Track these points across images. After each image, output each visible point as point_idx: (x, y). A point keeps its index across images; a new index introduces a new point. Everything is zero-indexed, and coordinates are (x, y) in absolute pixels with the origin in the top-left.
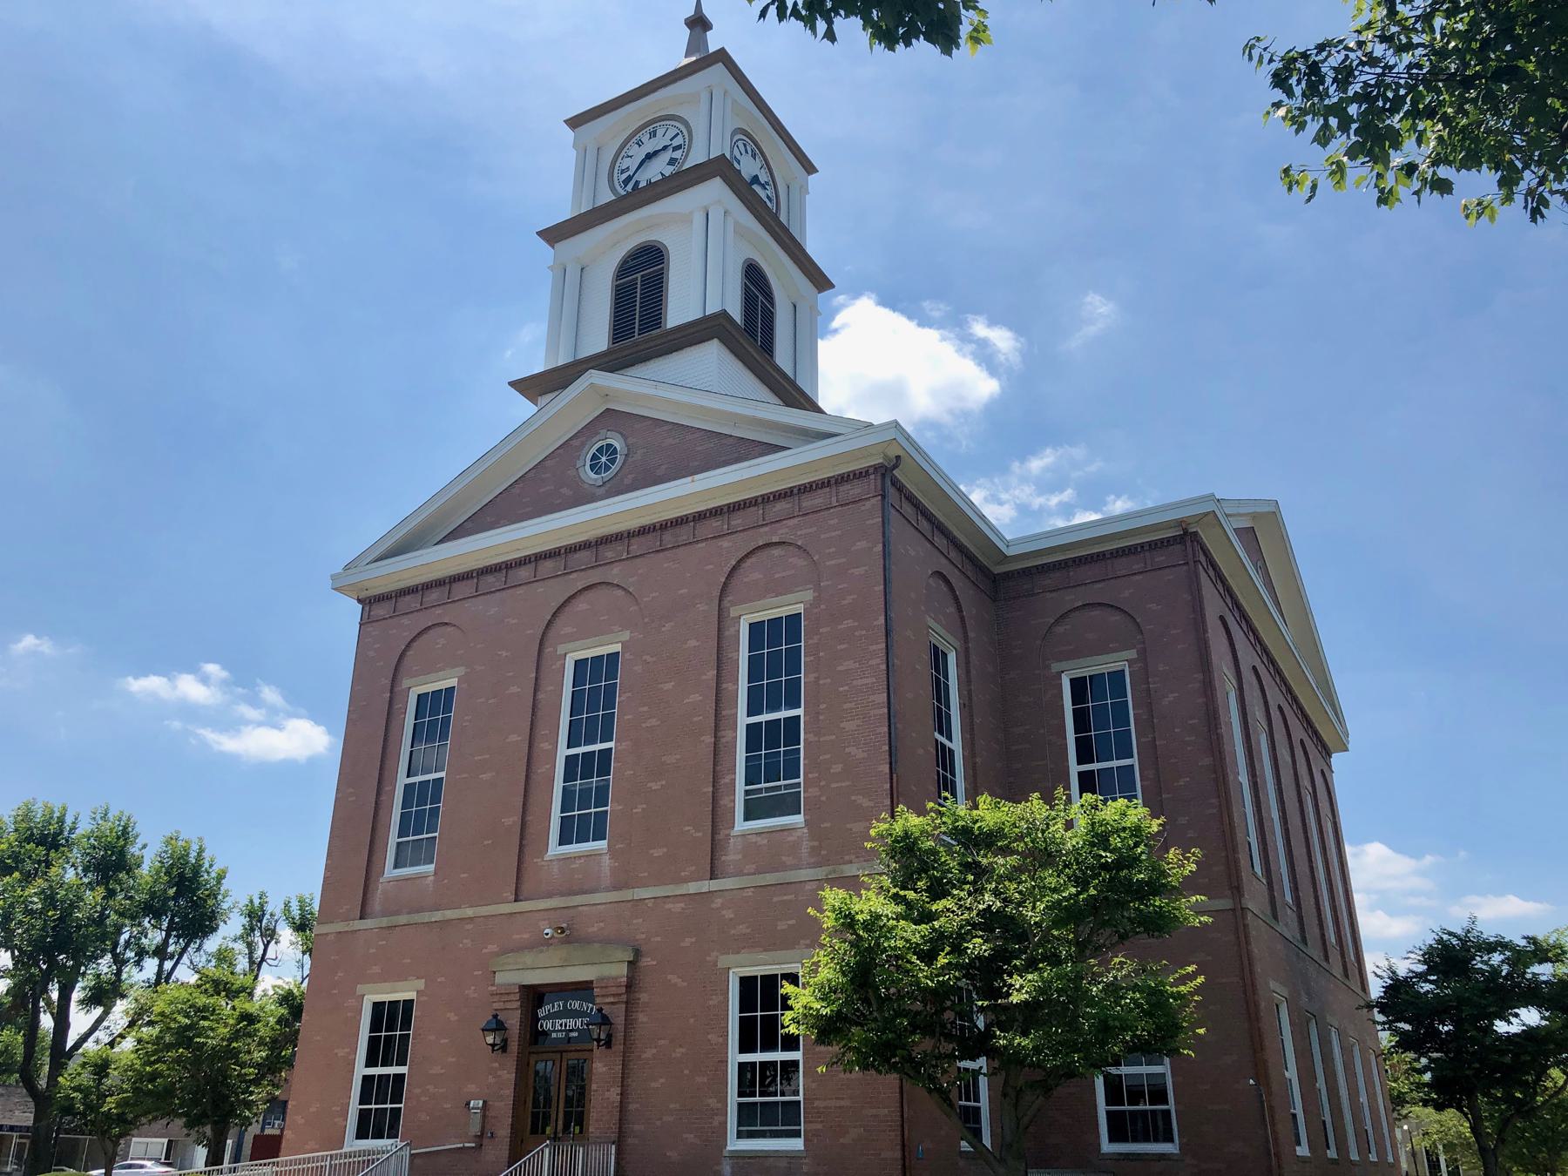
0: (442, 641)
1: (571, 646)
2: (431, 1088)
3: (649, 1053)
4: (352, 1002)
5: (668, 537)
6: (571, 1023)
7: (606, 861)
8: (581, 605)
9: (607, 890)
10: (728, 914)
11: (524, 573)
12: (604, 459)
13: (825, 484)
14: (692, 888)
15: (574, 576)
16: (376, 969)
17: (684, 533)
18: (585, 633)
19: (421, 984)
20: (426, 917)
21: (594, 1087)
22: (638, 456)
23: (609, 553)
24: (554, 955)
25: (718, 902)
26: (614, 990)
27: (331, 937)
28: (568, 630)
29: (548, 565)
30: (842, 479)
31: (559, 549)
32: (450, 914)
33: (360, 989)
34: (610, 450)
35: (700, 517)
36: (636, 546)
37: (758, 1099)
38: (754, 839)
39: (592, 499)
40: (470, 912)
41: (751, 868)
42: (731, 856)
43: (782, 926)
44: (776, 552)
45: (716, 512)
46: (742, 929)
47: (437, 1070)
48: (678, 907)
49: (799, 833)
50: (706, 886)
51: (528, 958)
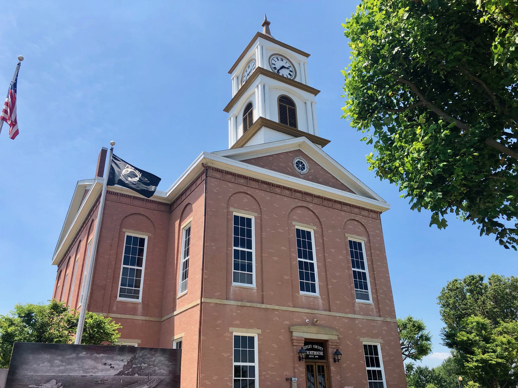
0: (246, 200)
1: (297, 223)
2: (270, 372)
3: (345, 365)
4: (227, 334)
5: (326, 203)
6: (315, 353)
7: (320, 301)
8: (299, 211)
9: (321, 310)
10: (360, 326)
11: (278, 190)
12: (300, 166)
13: (368, 210)
14: (350, 316)
15: (297, 200)
16: (238, 322)
17: (330, 204)
18: (301, 221)
19: (260, 331)
20: (255, 305)
21: (332, 375)
22: (312, 171)
23: (309, 199)
24: (314, 329)
25: (357, 322)
26: (335, 344)
27: (213, 305)
28: (294, 217)
29: (287, 192)
30: (372, 211)
31: (292, 189)
32: (269, 306)
33: (231, 329)
34: (298, 163)
35: (335, 201)
36: (316, 200)
37: (378, 381)
38: (361, 305)
39: (300, 178)
40: (277, 307)
41: (362, 313)
42: (357, 309)
43: (374, 332)
44: (356, 223)
45: (340, 203)
46: (364, 331)
47: (271, 365)
48: (346, 321)
49: (372, 306)
50: (354, 316)
51: (305, 329)
